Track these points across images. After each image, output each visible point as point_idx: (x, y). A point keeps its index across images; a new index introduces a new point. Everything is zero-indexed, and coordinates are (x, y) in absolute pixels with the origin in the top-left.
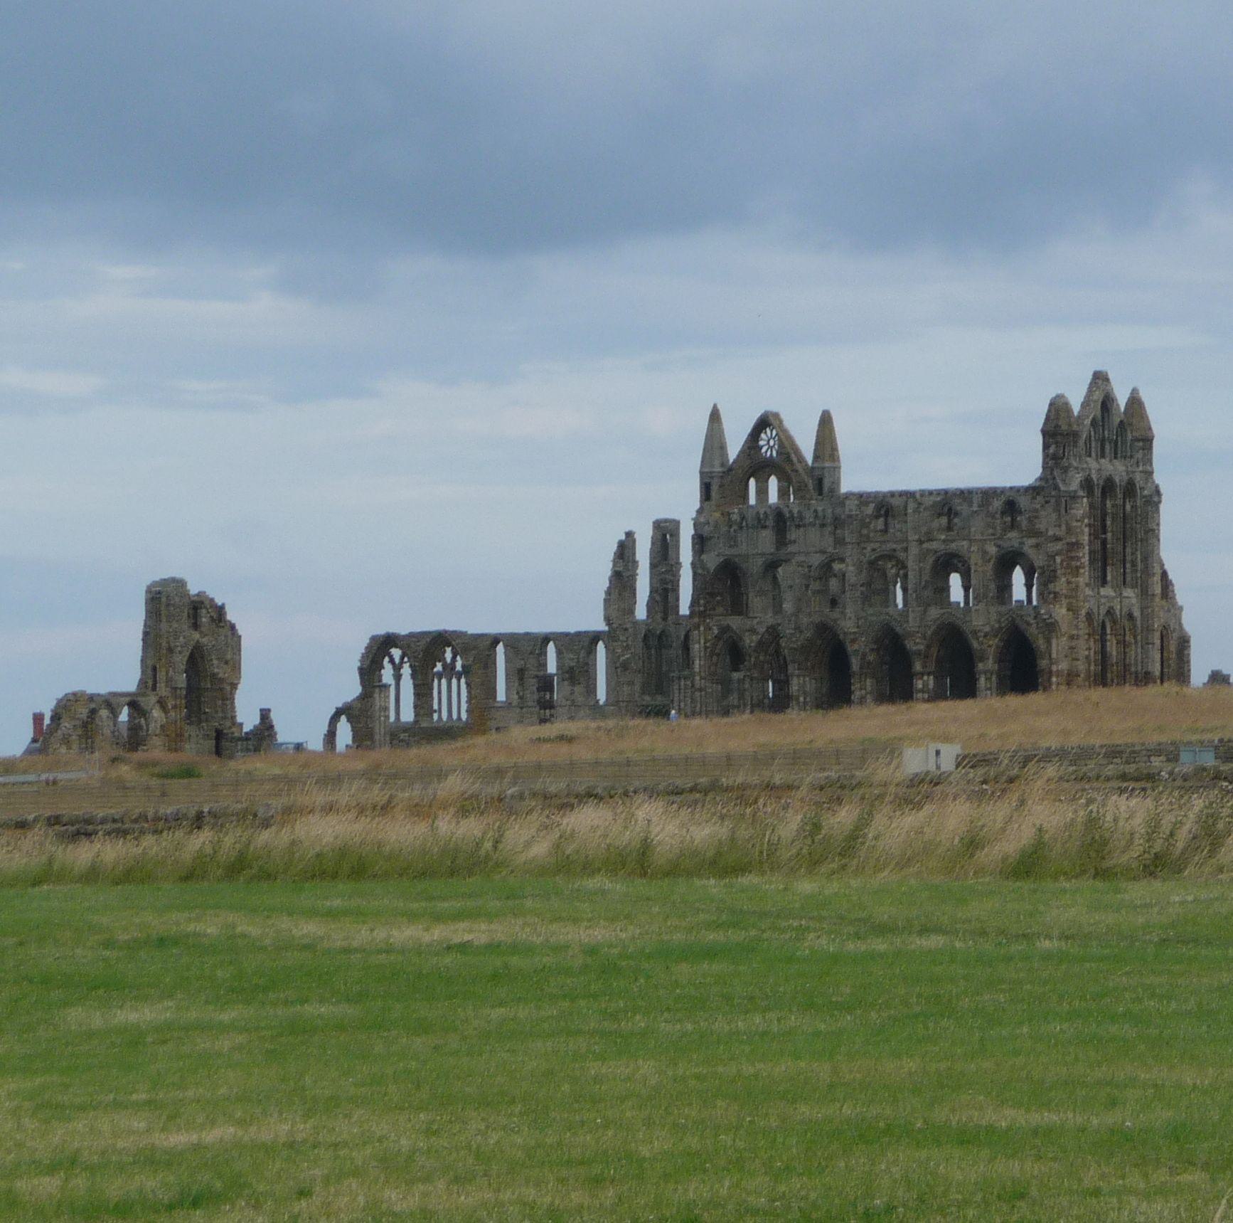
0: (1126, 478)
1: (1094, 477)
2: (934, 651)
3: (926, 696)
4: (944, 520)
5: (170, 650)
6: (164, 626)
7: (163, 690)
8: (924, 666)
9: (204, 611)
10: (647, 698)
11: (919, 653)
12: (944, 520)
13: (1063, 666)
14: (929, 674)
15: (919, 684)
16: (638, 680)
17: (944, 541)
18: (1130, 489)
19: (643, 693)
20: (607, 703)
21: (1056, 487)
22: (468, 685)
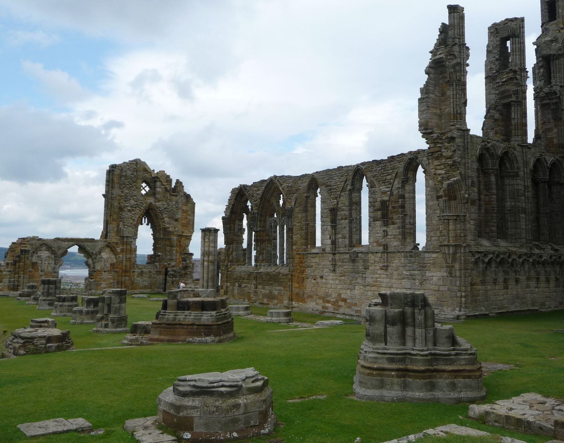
6: (116, 191)
7: (113, 238)
9: (158, 184)
10: (486, 243)
16: (472, 214)
19: (480, 234)
20: (427, 250)
22: (290, 230)
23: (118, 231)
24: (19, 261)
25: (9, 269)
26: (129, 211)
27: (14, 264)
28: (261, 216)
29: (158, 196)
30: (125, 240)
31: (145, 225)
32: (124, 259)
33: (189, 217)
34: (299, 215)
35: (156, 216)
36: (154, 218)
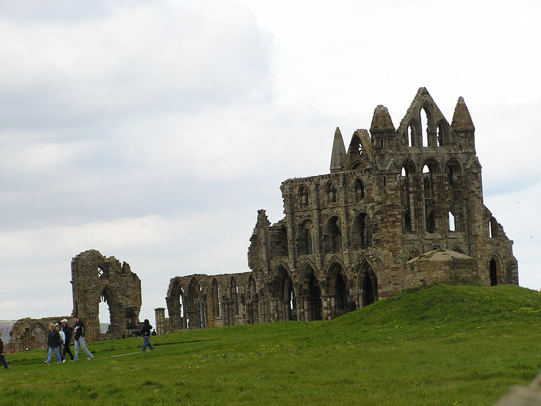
0: (447, 158)
1: (414, 159)
2: (333, 282)
3: (329, 311)
4: (331, 195)
5: (86, 292)
6: (81, 278)
8: (326, 292)
9: (110, 268)
11: (323, 283)
12: (331, 195)
13: (389, 288)
14: (330, 297)
15: (325, 304)
17: (331, 208)
18: (453, 166)
21: (377, 169)
23: (85, 309)
24: (25, 336)
25: (18, 342)
26: (92, 293)
27: (22, 339)
28: (190, 297)
29: (110, 278)
30: (91, 315)
31: (102, 301)
32: (92, 330)
33: (137, 293)
34: (209, 299)
35: (112, 294)
36: (110, 296)
